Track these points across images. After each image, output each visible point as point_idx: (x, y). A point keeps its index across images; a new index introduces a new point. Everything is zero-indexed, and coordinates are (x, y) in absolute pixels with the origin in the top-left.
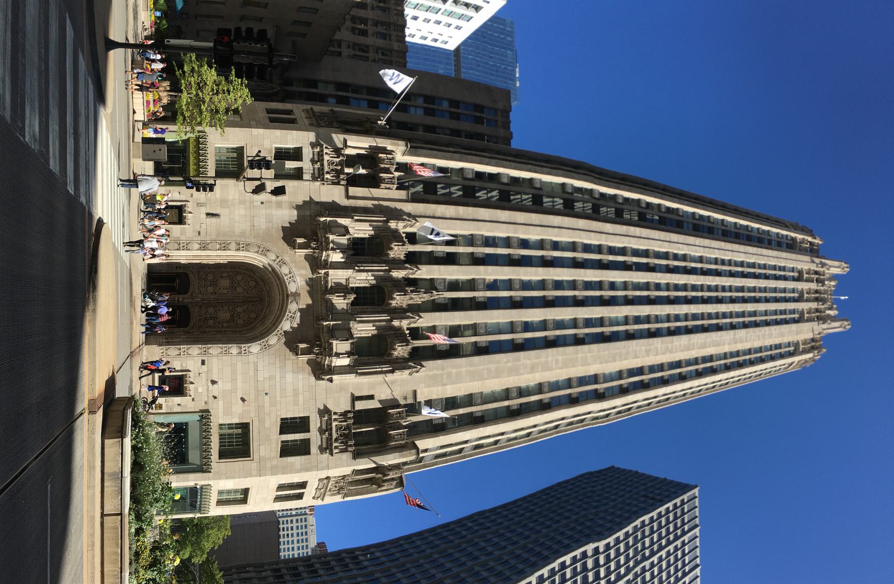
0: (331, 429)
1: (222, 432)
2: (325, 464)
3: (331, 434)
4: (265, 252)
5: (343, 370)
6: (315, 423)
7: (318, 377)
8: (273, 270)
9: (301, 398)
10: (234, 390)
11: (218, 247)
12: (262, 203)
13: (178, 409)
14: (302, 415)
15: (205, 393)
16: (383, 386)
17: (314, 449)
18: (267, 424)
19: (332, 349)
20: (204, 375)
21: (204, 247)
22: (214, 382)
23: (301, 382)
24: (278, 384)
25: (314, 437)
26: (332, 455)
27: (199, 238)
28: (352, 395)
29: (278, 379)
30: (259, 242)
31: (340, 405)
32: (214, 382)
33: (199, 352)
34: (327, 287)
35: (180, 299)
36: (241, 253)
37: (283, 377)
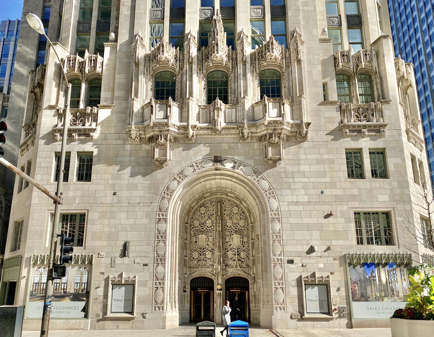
0: (359, 126)
1: (365, 240)
2: (395, 133)
3: (365, 127)
4: (169, 192)
5: (297, 110)
6: (350, 143)
7: (304, 138)
8: (189, 184)
9: (325, 157)
10: (320, 228)
11: (162, 244)
12: (115, 194)
13: (343, 289)
14: (344, 156)
15: (324, 260)
16: (311, 72)
17: (379, 144)
18: (355, 192)
19: (276, 122)
20: (305, 261)
21: (160, 260)
22: (311, 250)
23: (309, 156)
24: (312, 180)
25: (365, 144)
26: (385, 126)
27: (151, 265)
28: (321, 104)
29: (306, 180)
30: (159, 198)
31: (333, 116)
32: (311, 250)
33: (278, 266)
34: (207, 129)
35: (219, 287)
36: (170, 217)
37: (303, 174)
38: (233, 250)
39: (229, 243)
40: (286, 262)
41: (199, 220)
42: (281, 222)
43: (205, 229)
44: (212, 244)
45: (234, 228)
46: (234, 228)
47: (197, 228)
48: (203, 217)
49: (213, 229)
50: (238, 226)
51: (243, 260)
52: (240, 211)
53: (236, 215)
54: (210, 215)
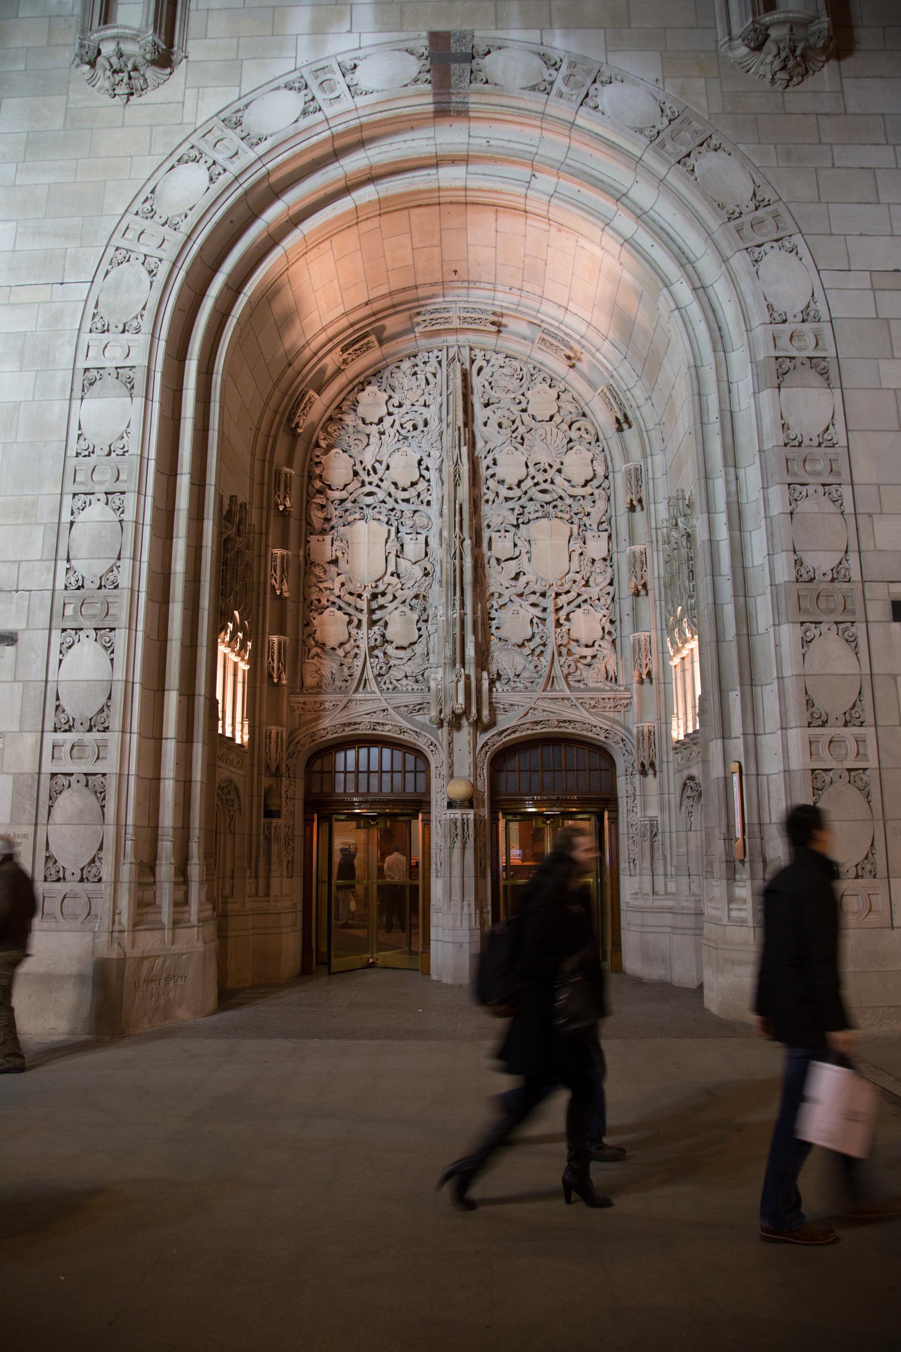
38: (533, 599)
39: (512, 567)
40: (879, 610)
41: (353, 452)
42: (835, 381)
43: (381, 495)
44: (418, 572)
45: (534, 492)
46: (534, 492)
47: (344, 495)
48: (374, 439)
49: (425, 497)
50: (559, 479)
51: (589, 652)
52: (568, 407)
53: (548, 426)
54: (409, 426)
